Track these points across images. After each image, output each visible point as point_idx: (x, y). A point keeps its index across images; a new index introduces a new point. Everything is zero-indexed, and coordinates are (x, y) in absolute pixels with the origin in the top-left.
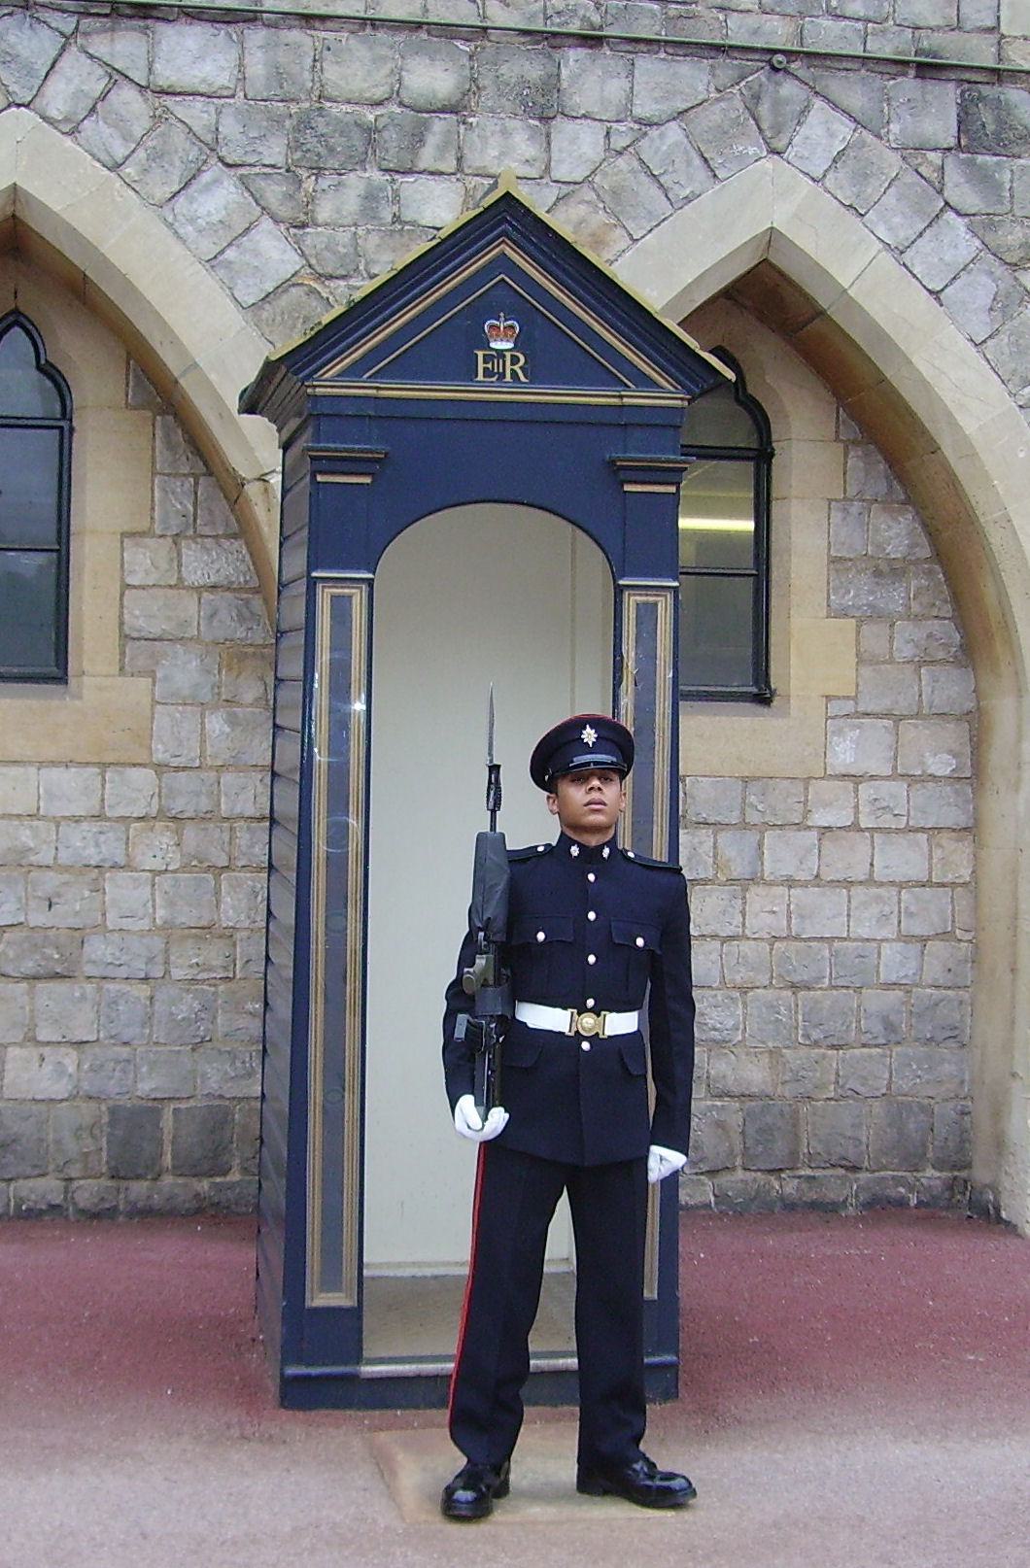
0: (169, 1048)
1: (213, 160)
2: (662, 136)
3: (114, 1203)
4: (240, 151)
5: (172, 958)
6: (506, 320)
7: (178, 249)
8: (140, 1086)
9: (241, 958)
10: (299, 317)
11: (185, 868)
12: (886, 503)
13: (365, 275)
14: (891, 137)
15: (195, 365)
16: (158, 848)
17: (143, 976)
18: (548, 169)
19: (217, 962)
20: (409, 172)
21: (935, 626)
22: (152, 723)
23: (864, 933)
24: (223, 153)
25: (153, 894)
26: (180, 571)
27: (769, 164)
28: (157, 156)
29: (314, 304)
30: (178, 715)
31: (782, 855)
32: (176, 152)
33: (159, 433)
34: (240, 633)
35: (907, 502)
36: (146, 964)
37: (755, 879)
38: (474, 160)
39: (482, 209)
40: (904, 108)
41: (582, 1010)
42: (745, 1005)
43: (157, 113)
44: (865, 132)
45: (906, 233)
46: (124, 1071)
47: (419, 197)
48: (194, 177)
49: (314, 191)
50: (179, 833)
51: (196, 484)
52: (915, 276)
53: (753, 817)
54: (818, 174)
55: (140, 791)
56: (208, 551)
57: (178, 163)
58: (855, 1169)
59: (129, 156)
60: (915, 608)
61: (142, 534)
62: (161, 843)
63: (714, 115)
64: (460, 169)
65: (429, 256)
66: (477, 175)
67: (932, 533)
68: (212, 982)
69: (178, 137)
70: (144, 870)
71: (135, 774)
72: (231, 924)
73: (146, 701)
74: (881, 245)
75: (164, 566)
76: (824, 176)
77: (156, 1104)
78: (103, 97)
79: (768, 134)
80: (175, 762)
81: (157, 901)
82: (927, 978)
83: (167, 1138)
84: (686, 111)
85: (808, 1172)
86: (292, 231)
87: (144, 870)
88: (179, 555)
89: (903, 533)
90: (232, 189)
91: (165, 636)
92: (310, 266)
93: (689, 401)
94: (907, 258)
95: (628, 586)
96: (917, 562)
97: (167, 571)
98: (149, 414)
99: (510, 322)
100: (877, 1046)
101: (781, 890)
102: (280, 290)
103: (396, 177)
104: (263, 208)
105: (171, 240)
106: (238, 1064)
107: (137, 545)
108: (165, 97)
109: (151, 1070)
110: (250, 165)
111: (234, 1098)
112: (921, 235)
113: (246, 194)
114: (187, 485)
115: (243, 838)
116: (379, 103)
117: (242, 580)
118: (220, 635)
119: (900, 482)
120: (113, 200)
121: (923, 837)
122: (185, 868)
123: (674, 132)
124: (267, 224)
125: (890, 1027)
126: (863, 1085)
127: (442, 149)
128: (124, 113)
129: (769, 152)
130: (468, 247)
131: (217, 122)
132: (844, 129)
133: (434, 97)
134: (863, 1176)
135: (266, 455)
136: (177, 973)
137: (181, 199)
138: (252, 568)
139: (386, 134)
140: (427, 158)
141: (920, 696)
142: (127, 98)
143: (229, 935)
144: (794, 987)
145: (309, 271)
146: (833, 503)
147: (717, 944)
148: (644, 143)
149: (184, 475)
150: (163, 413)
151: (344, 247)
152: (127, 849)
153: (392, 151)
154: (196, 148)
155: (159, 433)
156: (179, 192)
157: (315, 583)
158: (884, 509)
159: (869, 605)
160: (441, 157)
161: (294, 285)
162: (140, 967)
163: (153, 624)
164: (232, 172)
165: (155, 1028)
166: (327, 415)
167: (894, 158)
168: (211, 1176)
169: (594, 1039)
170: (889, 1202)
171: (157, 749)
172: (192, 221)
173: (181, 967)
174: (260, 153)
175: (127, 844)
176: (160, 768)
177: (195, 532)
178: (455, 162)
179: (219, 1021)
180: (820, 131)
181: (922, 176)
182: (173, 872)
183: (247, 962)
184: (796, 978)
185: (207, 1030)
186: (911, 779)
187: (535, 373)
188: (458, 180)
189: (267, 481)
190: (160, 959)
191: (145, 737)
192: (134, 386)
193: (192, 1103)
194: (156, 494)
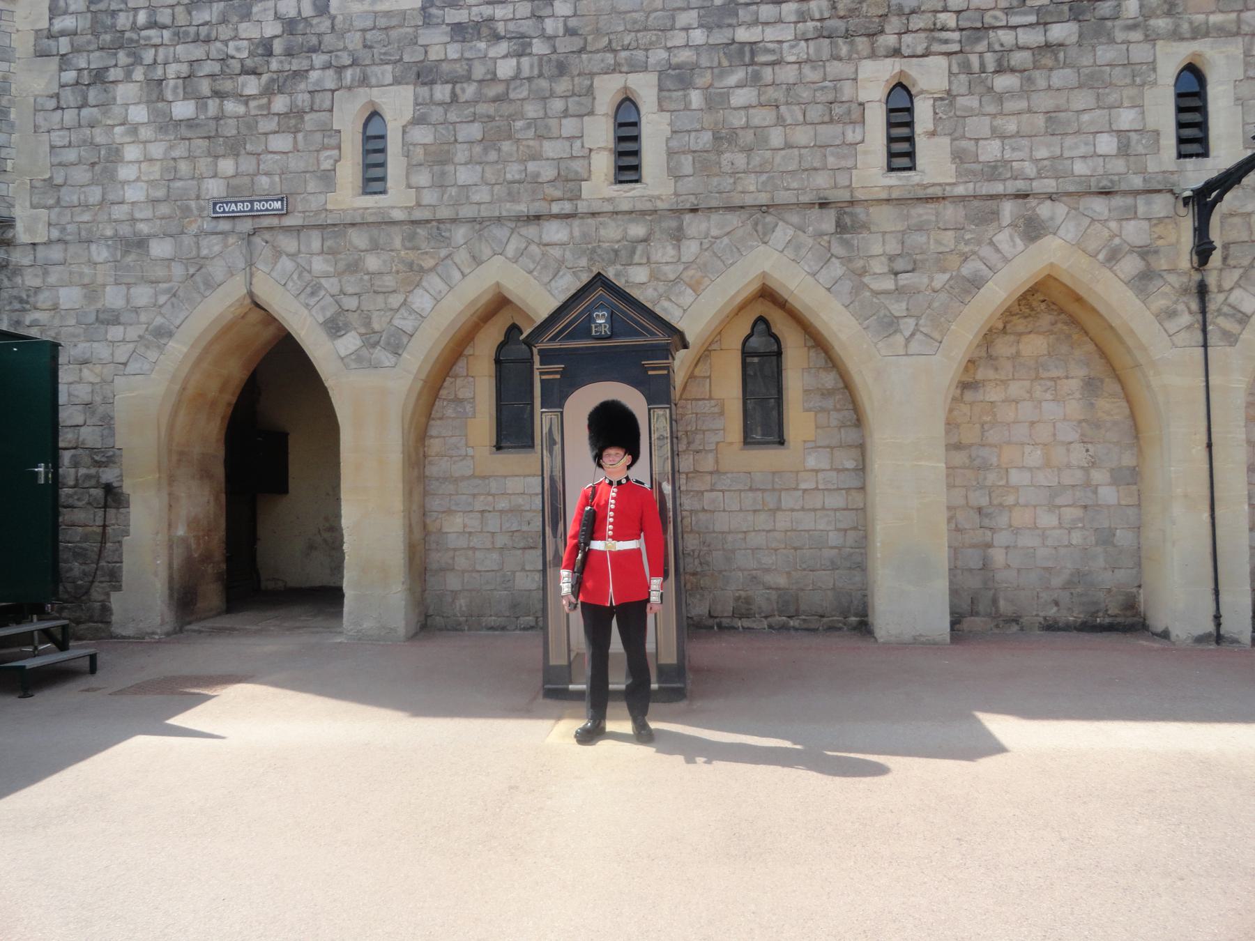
2: (721, 242)
18: (680, 259)
20: (630, 265)
21: (846, 412)
23: (821, 527)
27: (762, 247)
31: (788, 501)
37: (779, 509)
38: (654, 258)
42: (776, 555)
53: (777, 486)
58: (822, 616)
85: (804, 617)
96: (839, 389)
101: (790, 513)
116: (619, 241)
121: (844, 492)
123: (726, 240)
125: (832, 562)
134: (825, 620)
137: (553, 282)
140: (637, 259)
142: (534, 249)
144: (796, 549)
147: (765, 533)
148: (715, 246)
159: (820, 407)
172: (557, 288)
184: (795, 545)
186: (838, 471)
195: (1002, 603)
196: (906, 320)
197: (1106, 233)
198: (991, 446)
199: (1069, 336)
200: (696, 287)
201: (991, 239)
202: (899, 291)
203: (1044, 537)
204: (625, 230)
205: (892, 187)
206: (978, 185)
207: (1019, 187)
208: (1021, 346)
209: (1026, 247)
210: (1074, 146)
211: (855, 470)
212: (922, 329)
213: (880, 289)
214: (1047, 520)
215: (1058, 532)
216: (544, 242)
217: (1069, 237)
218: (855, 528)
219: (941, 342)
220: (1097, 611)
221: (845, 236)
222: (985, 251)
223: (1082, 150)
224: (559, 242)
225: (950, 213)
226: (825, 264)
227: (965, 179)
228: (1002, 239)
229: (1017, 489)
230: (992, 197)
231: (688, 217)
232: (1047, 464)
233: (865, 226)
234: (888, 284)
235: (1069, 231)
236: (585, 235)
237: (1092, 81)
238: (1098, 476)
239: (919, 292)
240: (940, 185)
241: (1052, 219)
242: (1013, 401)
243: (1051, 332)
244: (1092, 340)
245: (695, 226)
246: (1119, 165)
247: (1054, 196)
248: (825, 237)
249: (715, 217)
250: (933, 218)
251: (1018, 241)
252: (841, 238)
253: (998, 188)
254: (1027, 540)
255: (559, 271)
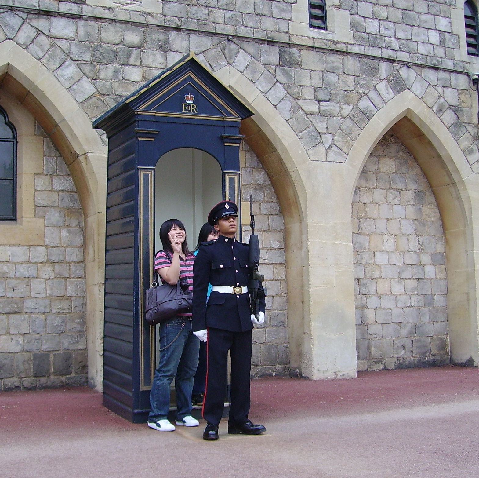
0: (51, 335)
1: (69, 59)
3: (36, 385)
4: (77, 56)
5: (52, 306)
6: (191, 95)
7: (59, 84)
8: (43, 347)
9: (74, 305)
10: (95, 107)
11: (55, 278)
12: (257, 168)
13: (114, 95)
14: (261, 61)
15: (64, 120)
16: (47, 272)
17: (43, 312)
19: (66, 307)
21: (272, 204)
22: (44, 233)
24: (72, 56)
25: (46, 286)
26: (52, 186)
27: (228, 67)
28: (52, 57)
29: (100, 102)
30: (53, 230)
32: (58, 55)
33: (45, 144)
34: (71, 205)
35: (263, 168)
36: (44, 308)
38: (145, 62)
39: (185, 62)
40: (264, 53)
41: (236, 286)
43: (52, 44)
44: (254, 59)
45: (266, 89)
46: (37, 342)
47: (130, 72)
48: (63, 63)
49: (99, 69)
50: (53, 267)
51: (57, 159)
52: (269, 101)
54: (242, 71)
55: (41, 254)
56: (61, 180)
57: (58, 59)
59: (43, 56)
60: (266, 199)
61: (40, 174)
62: (48, 270)
63: (213, 52)
64: (141, 65)
65: (169, 75)
66: (146, 67)
67: (270, 176)
68: (65, 314)
69: (58, 51)
70: (43, 279)
71: (39, 248)
72: (70, 295)
73: (43, 226)
74: (260, 92)
75: (47, 184)
76: (244, 71)
77: (48, 353)
78: (35, 38)
79: (228, 59)
80: (52, 245)
81: (47, 288)
82: (275, 308)
83: (52, 363)
84: (205, 51)
86: (92, 81)
87: (43, 279)
88: (52, 181)
89: (262, 177)
90: (75, 67)
91: (48, 206)
92: (98, 91)
93: (242, 120)
94: (267, 95)
95: (227, 172)
96: (266, 186)
97: (48, 186)
98: (42, 138)
99: (191, 96)
100: (262, 328)
102: (89, 98)
103: (123, 66)
104: (84, 74)
105: (57, 81)
106: (73, 339)
107: (39, 178)
108: (54, 39)
109: (46, 342)
110: (80, 61)
111: (72, 350)
112: (270, 89)
113: (79, 69)
114: (54, 160)
115: (73, 268)
116: (118, 44)
117: (71, 189)
118: (65, 206)
119: (262, 163)
120: (39, 69)
121: (271, 266)
122: (55, 278)
124: (85, 78)
126: (258, 340)
127: (136, 59)
128: (42, 43)
129: (228, 64)
130: (180, 73)
131: (70, 48)
132: (249, 58)
133: (134, 43)
134: (259, 367)
135: (86, 147)
136: (54, 311)
137: (59, 70)
138: (74, 185)
139: (120, 53)
140: (132, 61)
141: (269, 224)
142: (42, 39)
143: (70, 298)
145: (98, 93)
146: (242, 169)
149: (53, 156)
150: (46, 137)
151: (108, 86)
152: (37, 272)
153: (121, 58)
154: (64, 55)
155: (45, 144)
156: (58, 68)
157: (138, 170)
158: (256, 170)
160: (136, 61)
161: (93, 97)
162: (42, 309)
163: (44, 201)
164: (75, 62)
165: (47, 329)
166: (141, 120)
167: (263, 67)
168: (66, 375)
169: (240, 295)
170: (267, 375)
171: (46, 241)
172: (63, 76)
173: (55, 309)
174: (83, 57)
175: (37, 270)
176: (47, 246)
177: (57, 174)
178: (140, 63)
179: (67, 326)
180: (242, 58)
181: (270, 72)
182: (52, 279)
183: (75, 307)
185: (63, 329)
187: (199, 110)
188: (141, 68)
189: (87, 155)
190: (48, 306)
191: (42, 237)
192: (37, 129)
193: (59, 352)
194: (44, 162)
195: (373, 349)
196: (326, 135)
197: (437, 94)
198: (364, 235)
199: (406, 162)
201: (375, 86)
202: (320, 113)
203: (397, 301)
204: (123, 36)
205: (315, 38)
206: (367, 48)
207: (390, 54)
208: (380, 165)
209: (395, 95)
210: (419, 34)
211: (279, 249)
212: (336, 143)
213: (309, 110)
214: (398, 289)
215: (405, 297)
216: (53, 35)
217: (418, 93)
218: (279, 295)
219: (347, 154)
220: (426, 353)
221: (286, 68)
222: (372, 94)
223: (423, 38)
224: (65, 37)
225: (352, 64)
226: (273, 86)
227: (358, 42)
228: (382, 86)
229: (380, 266)
230: (375, 58)
231: (173, 34)
232: (397, 250)
233: (299, 64)
234: (314, 108)
235: (418, 88)
236: (88, 34)
238: (426, 259)
239: (333, 117)
240: (345, 43)
241: (408, 79)
242: (377, 203)
243: (397, 158)
244: (419, 166)
246: (440, 52)
247: (409, 64)
248: (272, 67)
249: (194, 38)
250: (341, 66)
251: (391, 91)
252: (283, 69)
253: (377, 52)
254: (387, 303)
255: (65, 61)
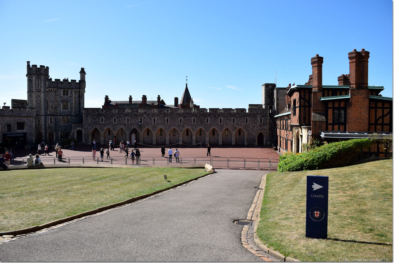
200: (118, 128)
225: (130, 125)
237: (136, 119)
245: (118, 125)
